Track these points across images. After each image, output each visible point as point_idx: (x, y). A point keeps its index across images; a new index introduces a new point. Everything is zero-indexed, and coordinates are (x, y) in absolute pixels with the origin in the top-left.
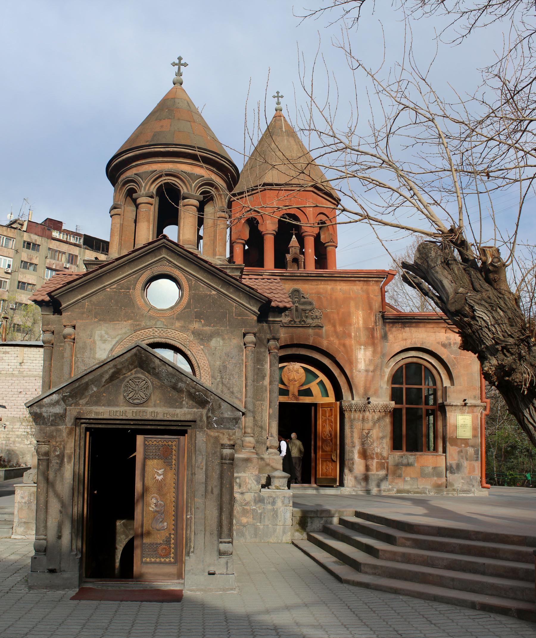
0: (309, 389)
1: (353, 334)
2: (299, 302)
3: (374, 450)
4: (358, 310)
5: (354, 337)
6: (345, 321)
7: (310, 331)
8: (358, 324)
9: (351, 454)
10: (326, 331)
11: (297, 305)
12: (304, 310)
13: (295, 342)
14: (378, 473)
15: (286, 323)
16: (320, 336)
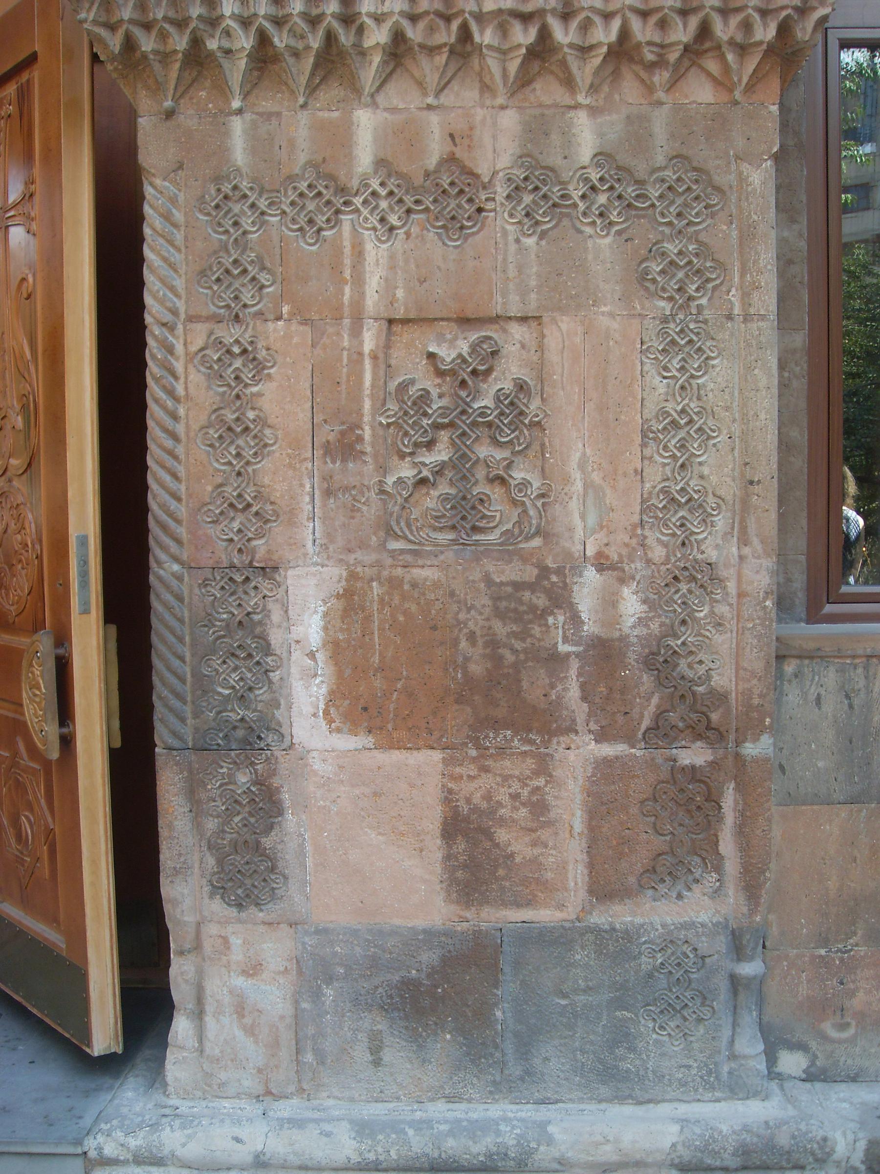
3: (561, 599)
9: (228, 679)
14: (621, 915)
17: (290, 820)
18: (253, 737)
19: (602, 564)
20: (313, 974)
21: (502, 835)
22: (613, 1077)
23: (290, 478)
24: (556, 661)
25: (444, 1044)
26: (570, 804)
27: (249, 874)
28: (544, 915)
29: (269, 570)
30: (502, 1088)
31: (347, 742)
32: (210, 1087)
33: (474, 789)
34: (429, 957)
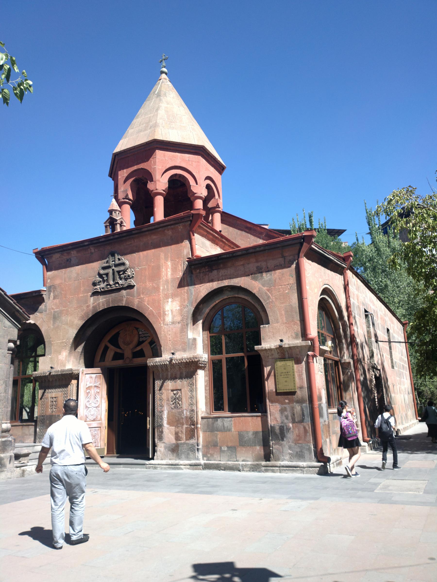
0: (142, 350)
1: (161, 288)
2: (116, 266)
3: (183, 413)
4: (167, 261)
5: (163, 289)
6: (156, 275)
7: (124, 292)
8: (167, 276)
10: (137, 289)
11: (113, 268)
12: (119, 272)
13: (111, 306)
14: (188, 442)
15: (103, 288)
16: (133, 296)
17: (164, 433)
18: (161, 426)
19: (186, 410)
20: (165, 448)
21: (179, 434)
22: (188, 458)
23: (165, 403)
24: (182, 418)
25: (175, 454)
26: (184, 431)
27: (161, 438)
28: (182, 442)
29: (163, 411)
30: (179, 459)
31: (168, 426)
32: (157, 459)
33: (177, 430)
34: (174, 446)
